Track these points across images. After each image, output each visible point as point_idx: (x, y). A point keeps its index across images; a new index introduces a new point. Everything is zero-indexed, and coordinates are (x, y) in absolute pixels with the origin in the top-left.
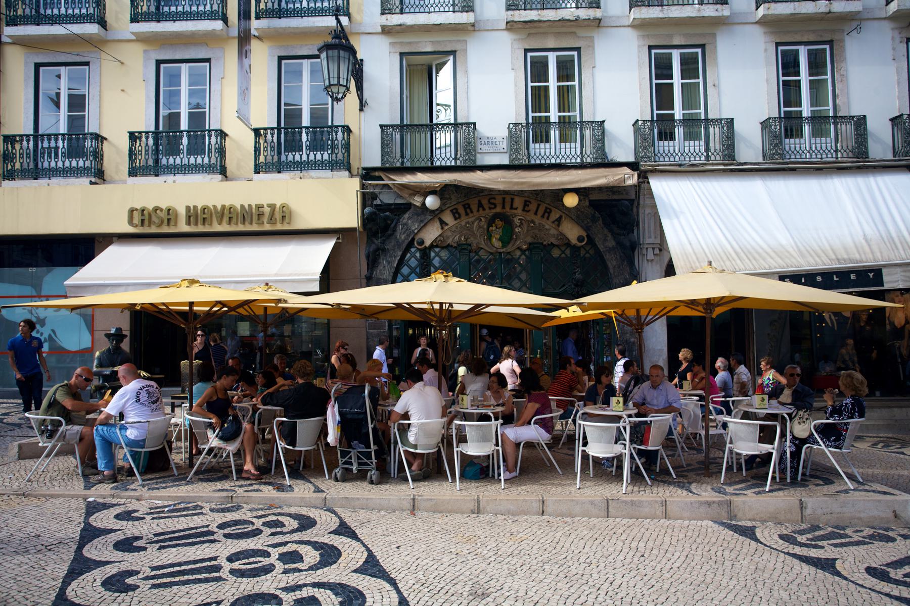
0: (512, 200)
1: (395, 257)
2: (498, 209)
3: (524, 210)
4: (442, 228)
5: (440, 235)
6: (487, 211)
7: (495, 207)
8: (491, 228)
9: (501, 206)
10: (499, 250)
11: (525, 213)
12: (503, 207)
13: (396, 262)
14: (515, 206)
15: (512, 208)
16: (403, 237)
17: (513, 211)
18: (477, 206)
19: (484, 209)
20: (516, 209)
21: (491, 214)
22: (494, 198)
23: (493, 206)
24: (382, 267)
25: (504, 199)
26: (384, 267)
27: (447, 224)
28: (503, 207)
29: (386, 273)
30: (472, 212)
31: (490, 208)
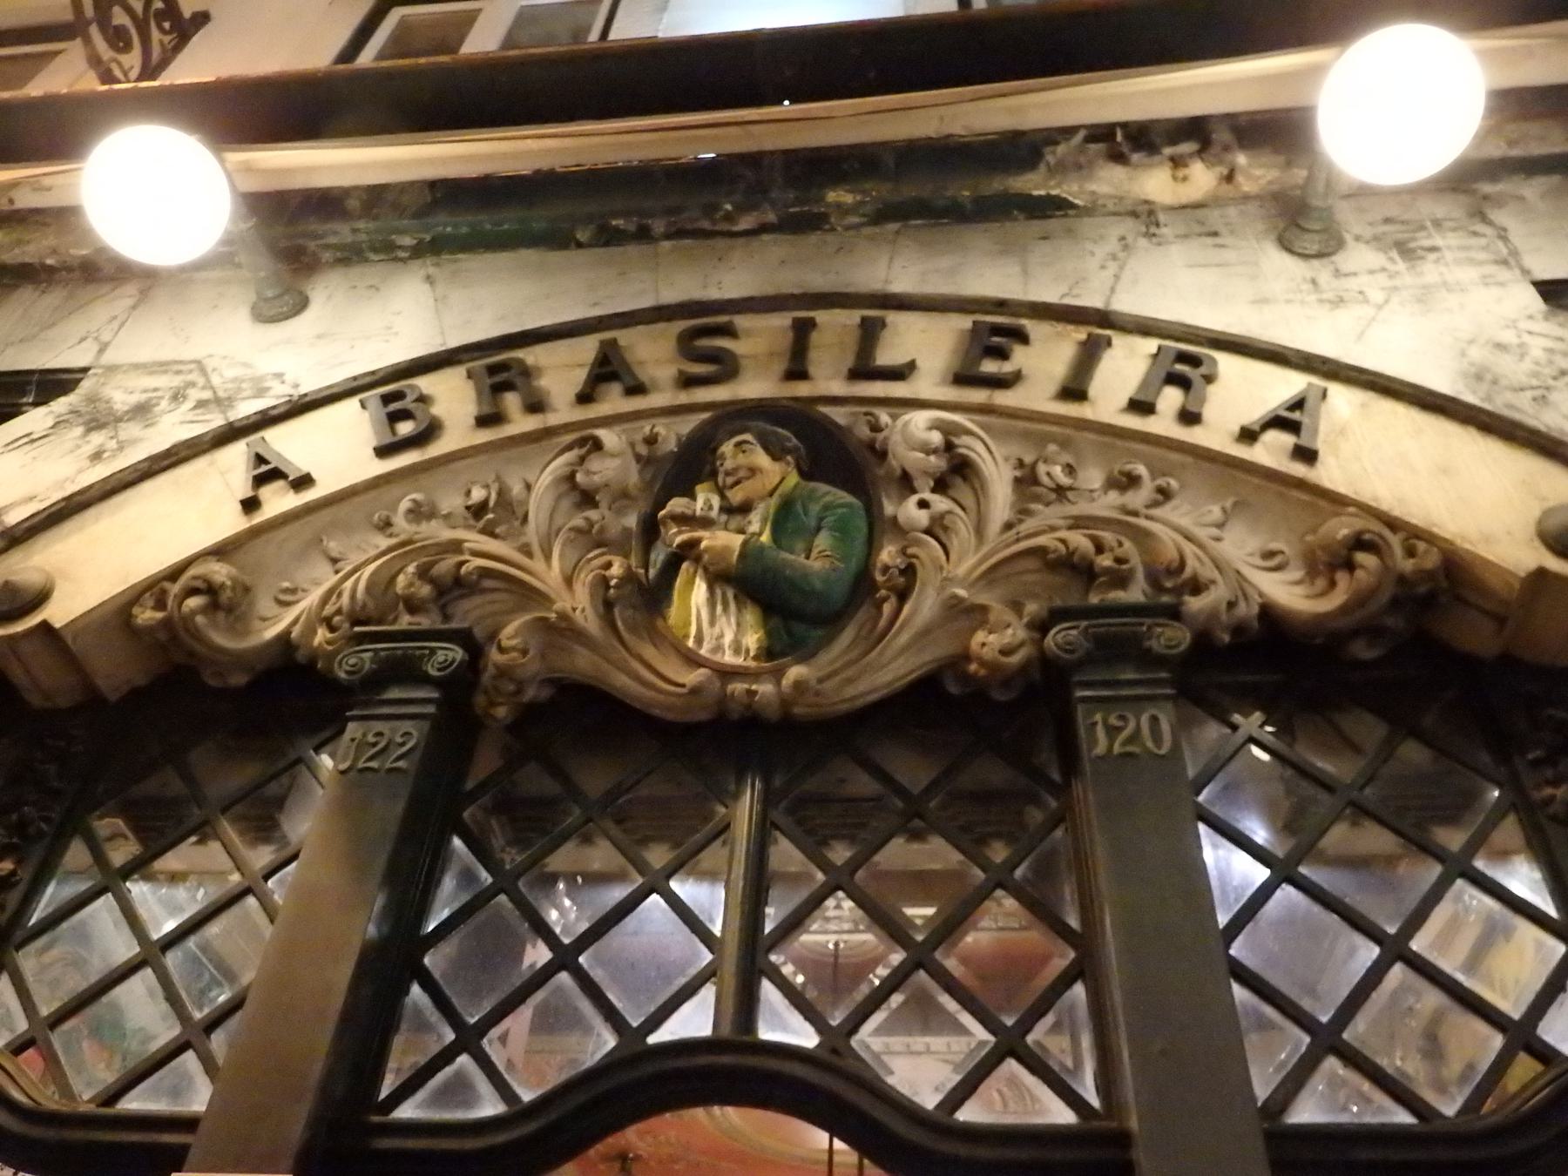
0: (870, 333)
2: (754, 386)
3: (964, 378)
5: (220, 551)
7: (727, 368)
8: (677, 505)
9: (780, 366)
10: (738, 687)
11: (978, 396)
12: (797, 372)
14: (887, 356)
15: (864, 370)
18: (580, 376)
21: (687, 425)
22: (728, 331)
25: (803, 329)
28: (797, 372)
30: (535, 406)
31: (688, 382)
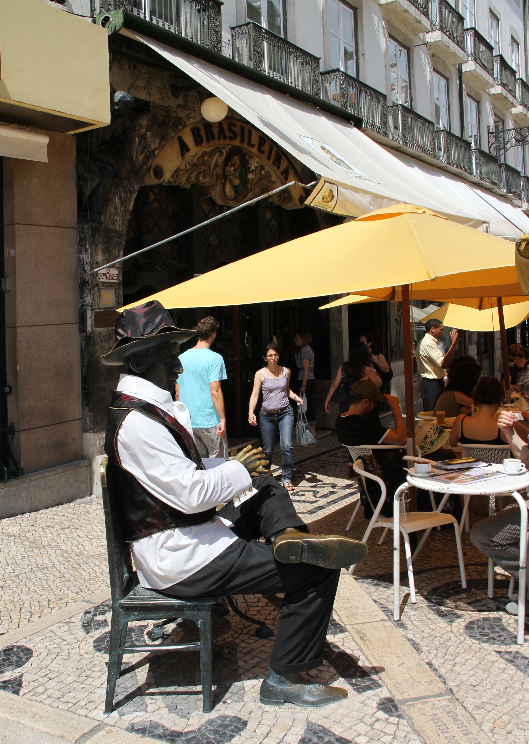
1: (131, 192)
4: (183, 154)
6: (227, 140)
13: (133, 202)
16: (141, 158)
17: (250, 149)
19: (225, 138)
20: (253, 146)
23: (232, 136)
24: (112, 209)
26: (116, 209)
27: (188, 150)
28: (242, 141)
29: (119, 219)
30: (213, 138)
31: (230, 138)
